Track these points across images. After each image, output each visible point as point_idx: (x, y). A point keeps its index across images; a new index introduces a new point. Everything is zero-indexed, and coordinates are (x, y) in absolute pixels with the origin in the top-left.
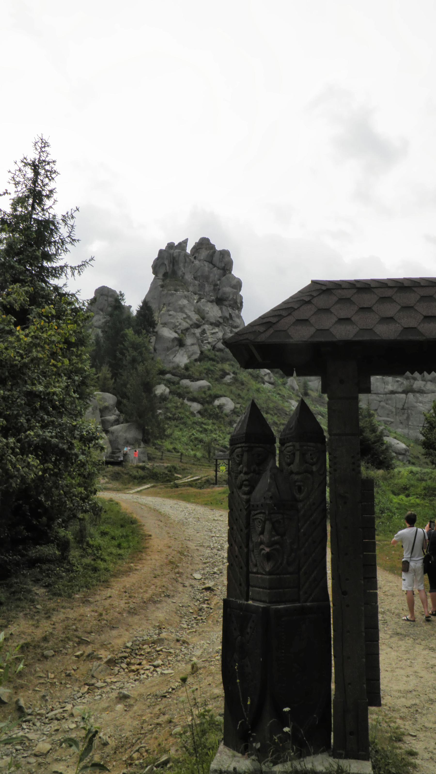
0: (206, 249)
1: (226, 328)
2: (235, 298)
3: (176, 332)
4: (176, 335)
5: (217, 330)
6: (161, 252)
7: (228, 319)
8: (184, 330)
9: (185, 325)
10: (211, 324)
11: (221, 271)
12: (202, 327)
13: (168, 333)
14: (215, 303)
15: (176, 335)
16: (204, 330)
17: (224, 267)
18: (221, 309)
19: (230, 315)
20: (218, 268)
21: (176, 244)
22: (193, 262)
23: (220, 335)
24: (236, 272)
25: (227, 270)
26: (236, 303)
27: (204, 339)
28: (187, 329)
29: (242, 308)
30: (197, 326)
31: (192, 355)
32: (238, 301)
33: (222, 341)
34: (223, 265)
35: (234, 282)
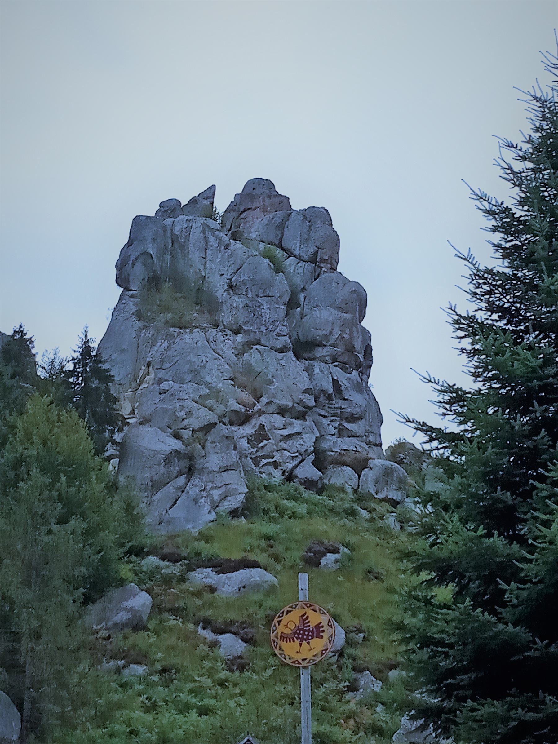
0: (265, 211)
1: (325, 422)
2: (346, 336)
3: (177, 436)
4: (177, 445)
5: (297, 426)
6: (139, 223)
7: (330, 398)
8: (201, 429)
9: (203, 416)
10: (282, 411)
11: (309, 266)
12: (254, 421)
13: (155, 442)
14: (291, 354)
15: (177, 445)
16: (262, 427)
17: (316, 253)
18: (309, 370)
19: (335, 382)
20: (300, 258)
21: (184, 202)
22: (227, 247)
23: (308, 441)
24: (348, 266)
25: (324, 261)
26: (351, 349)
27: (261, 453)
28: (209, 428)
29: (370, 367)
30: (243, 419)
31: (224, 497)
32: (358, 345)
33: (312, 457)
34: (312, 250)
35: (343, 294)
